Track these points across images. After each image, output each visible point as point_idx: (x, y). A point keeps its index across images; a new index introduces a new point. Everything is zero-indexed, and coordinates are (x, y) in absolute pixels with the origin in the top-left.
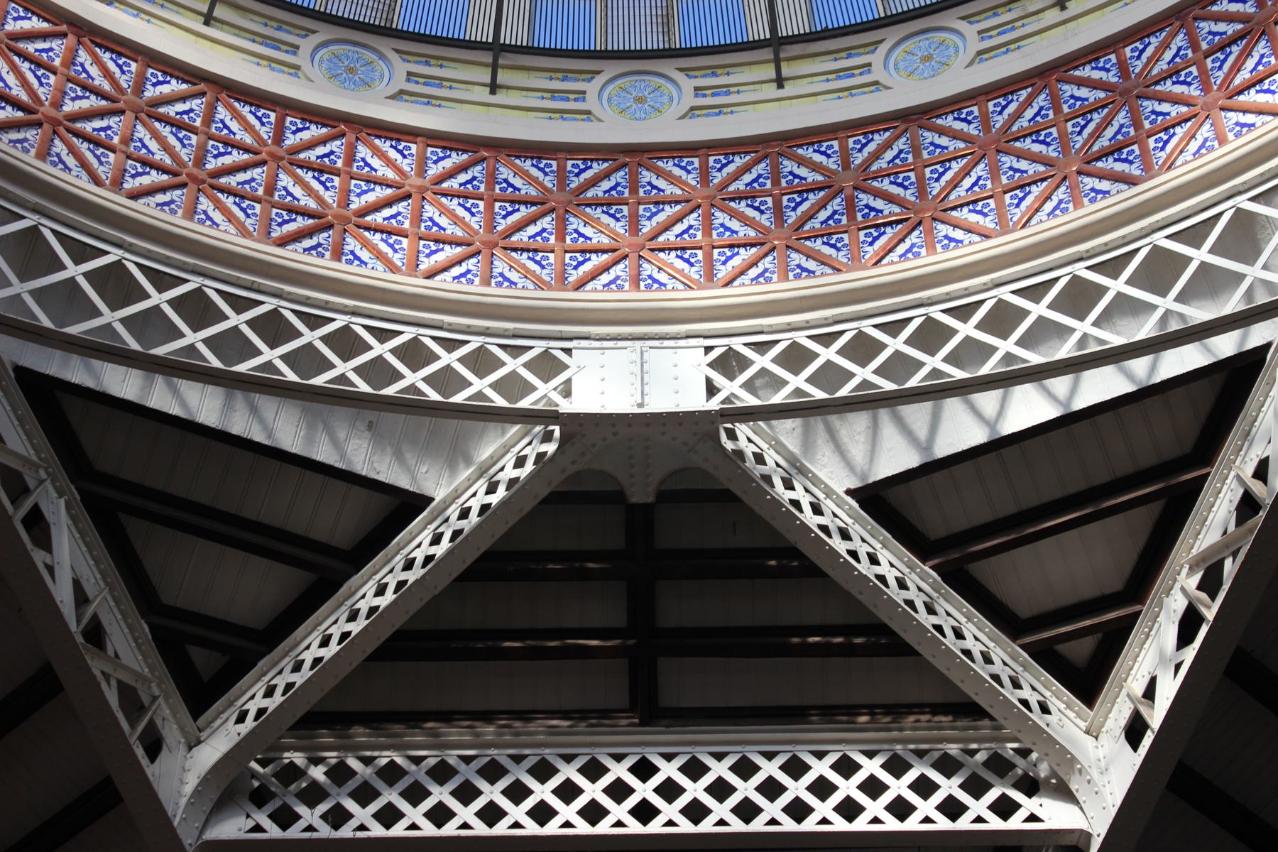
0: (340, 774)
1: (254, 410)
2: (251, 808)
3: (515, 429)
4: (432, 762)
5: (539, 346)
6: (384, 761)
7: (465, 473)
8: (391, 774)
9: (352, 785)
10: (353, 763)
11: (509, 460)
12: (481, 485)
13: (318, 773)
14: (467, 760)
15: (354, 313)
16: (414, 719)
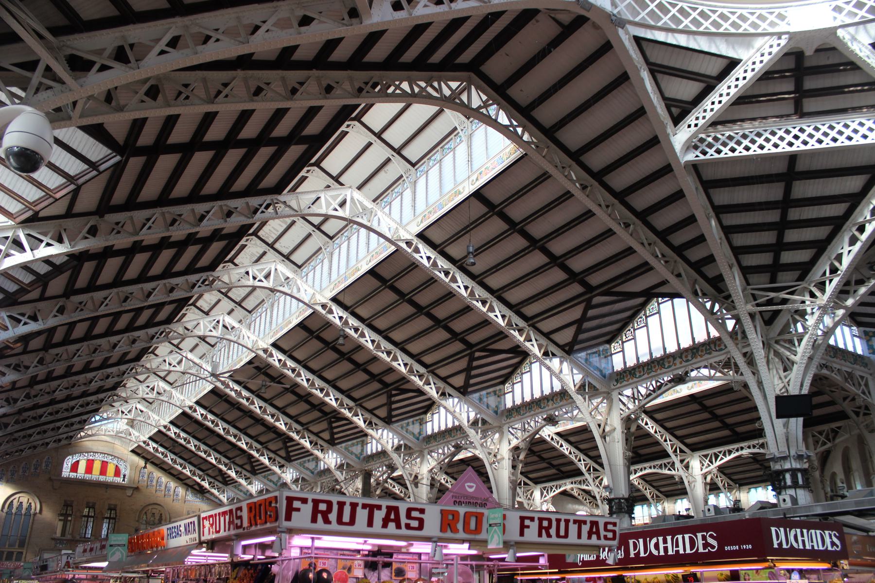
0: (716, 139)
1: (695, 40)
2: (694, 151)
3: (767, 38)
4: (741, 134)
5: (777, 11)
6: (727, 135)
7: (752, 51)
8: (730, 138)
9: (720, 142)
10: (719, 136)
11: (767, 45)
12: (759, 54)
13: (710, 139)
14: (751, 132)
15: (724, 7)
16: (734, 122)
